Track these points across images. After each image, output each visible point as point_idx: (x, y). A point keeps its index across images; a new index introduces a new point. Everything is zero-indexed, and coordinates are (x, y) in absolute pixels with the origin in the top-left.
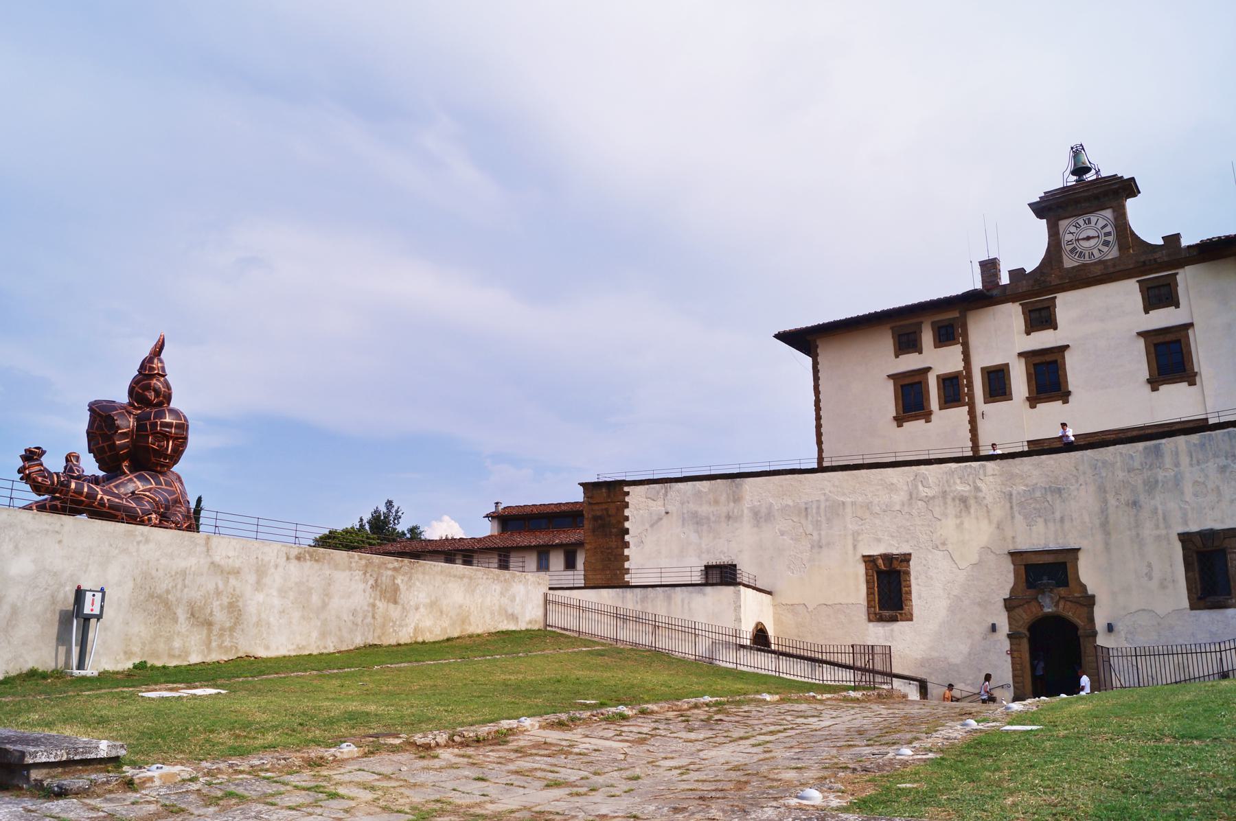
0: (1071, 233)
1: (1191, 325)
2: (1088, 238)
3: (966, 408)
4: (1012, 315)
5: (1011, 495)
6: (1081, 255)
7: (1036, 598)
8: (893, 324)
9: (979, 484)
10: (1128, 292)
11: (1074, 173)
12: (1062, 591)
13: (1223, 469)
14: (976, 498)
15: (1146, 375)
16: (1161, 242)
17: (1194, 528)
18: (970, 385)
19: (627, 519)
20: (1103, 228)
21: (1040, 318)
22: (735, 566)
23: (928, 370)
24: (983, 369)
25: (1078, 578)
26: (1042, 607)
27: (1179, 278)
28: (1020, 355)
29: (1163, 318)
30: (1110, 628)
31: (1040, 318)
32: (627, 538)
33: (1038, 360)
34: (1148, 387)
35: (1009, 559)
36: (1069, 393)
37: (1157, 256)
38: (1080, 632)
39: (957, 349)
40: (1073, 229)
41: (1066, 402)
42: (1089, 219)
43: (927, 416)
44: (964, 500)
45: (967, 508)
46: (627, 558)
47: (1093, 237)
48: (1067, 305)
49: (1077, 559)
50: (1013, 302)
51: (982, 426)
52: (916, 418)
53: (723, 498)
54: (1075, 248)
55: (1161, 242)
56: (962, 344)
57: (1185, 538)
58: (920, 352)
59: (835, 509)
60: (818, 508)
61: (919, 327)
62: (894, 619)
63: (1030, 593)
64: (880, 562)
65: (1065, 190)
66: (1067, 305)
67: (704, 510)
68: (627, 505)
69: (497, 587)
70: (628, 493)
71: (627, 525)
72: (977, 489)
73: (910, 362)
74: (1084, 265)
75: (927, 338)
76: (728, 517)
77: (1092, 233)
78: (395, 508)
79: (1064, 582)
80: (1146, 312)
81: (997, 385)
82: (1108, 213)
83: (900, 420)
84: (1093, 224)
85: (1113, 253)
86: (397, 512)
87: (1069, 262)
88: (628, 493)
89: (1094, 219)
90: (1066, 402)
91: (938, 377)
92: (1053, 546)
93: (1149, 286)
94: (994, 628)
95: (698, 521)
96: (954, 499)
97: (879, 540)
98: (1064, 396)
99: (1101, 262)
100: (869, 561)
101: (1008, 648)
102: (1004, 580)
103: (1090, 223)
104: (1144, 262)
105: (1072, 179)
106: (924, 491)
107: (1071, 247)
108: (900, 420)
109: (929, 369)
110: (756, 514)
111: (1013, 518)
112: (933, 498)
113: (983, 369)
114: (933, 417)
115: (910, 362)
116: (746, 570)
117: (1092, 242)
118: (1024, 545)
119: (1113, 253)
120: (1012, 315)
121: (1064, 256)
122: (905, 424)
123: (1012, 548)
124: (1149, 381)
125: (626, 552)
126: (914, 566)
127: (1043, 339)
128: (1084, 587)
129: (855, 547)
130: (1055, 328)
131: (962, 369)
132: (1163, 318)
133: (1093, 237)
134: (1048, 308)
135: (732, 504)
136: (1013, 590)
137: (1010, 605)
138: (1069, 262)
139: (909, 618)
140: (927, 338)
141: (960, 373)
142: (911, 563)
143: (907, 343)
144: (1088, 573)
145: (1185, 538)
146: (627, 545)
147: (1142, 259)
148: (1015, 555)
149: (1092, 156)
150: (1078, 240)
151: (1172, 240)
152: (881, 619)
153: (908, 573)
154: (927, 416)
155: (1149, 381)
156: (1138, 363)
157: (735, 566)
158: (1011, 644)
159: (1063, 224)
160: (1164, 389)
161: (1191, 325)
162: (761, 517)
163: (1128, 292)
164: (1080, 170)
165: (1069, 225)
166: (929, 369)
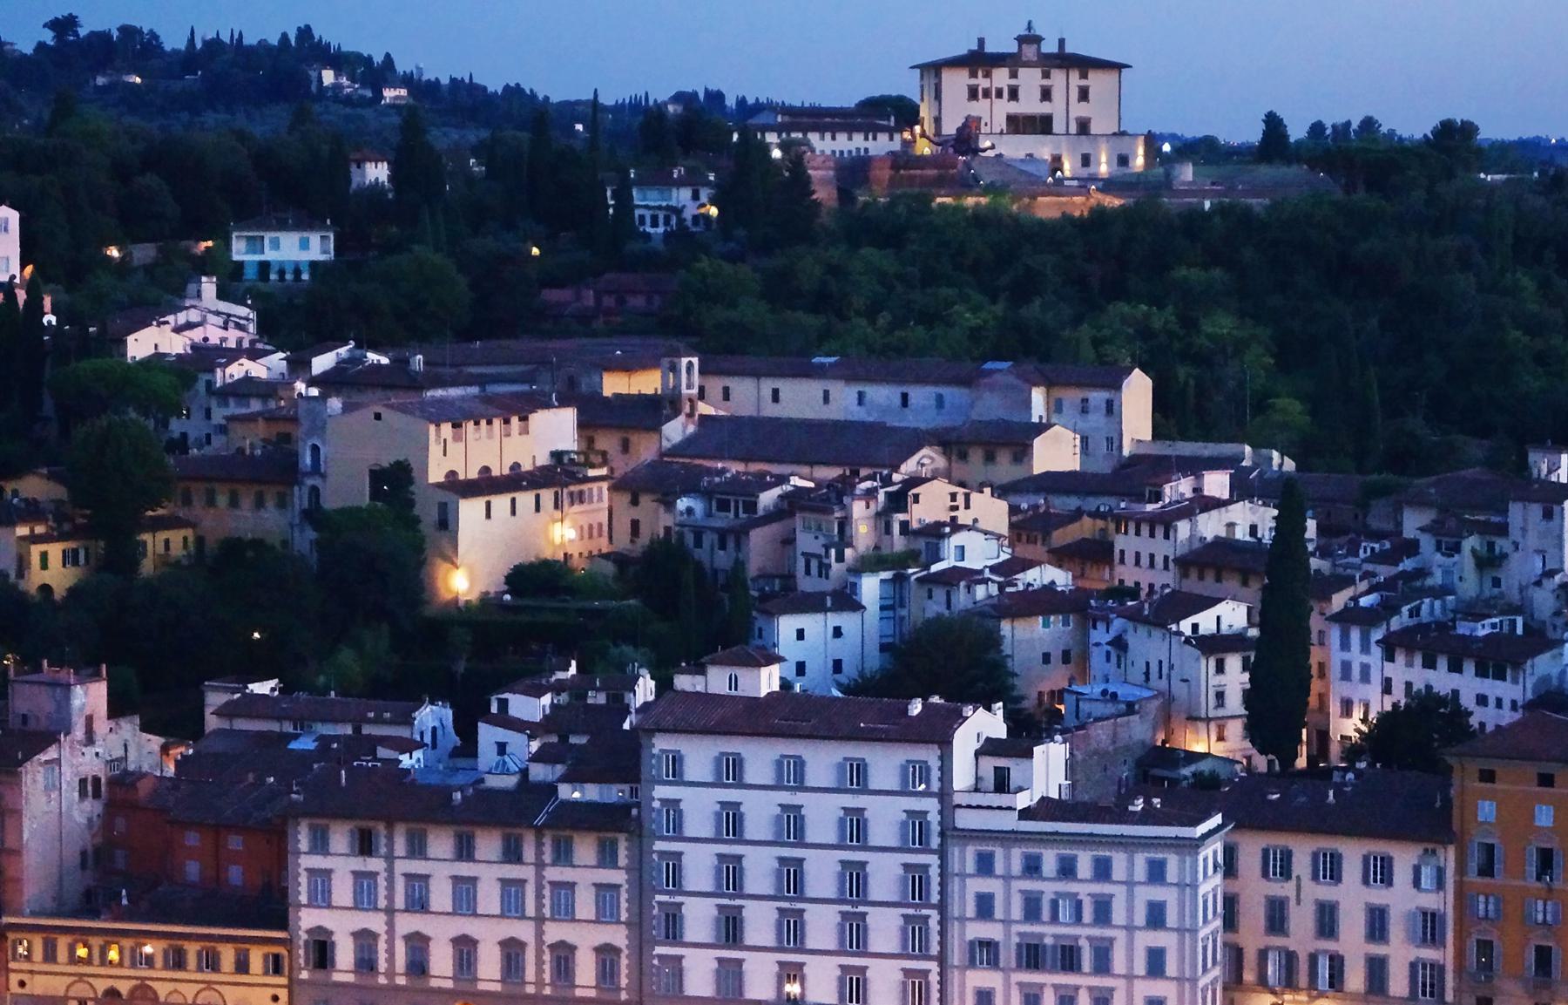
10: (1037, 72)
15: (1039, 97)
21: (1014, 75)
23: (978, 85)
29: (1046, 82)
31: (1014, 75)
48: (1022, 72)
65: (1026, 36)
66: (1022, 72)
73: (973, 81)
81: (999, 94)
82: (1036, 46)
87: (1024, 59)
98: (1017, 100)
105: (1027, 33)
115: (973, 81)
127: (1013, 82)
132: (1046, 82)
138: (1024, 59)
140: (980, 73)
143: (973, 75)
149: (1034, 24)
156: (1038, 95)
163: (1037, 72)
164: (1029, 28)
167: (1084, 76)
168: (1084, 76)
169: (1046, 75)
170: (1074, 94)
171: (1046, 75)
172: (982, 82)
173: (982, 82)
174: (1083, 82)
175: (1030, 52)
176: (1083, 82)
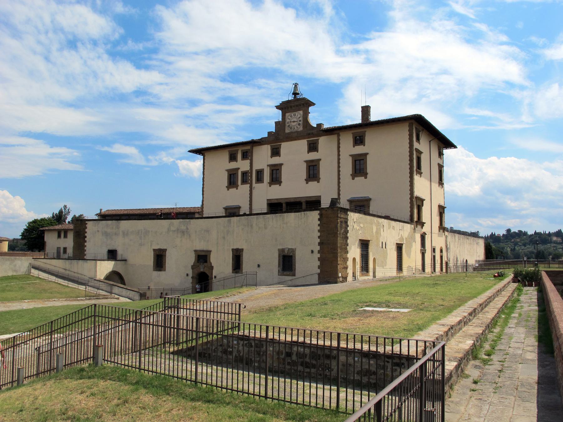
0: (289, 119)
1: (320, 160)
2: (294, 122)
3: (249, 185)
4: (266, 149)
5: (196, 231)
6: (291, 128)
7: (199, 266)
8: (228, 150)
9: (188, 227)
10: (303, 144)
11: (293, 94)
12: (206, 264)
13: (243, 229)
14: (187, 231)
15: (305, 176)
16: (315, 126)
17: (235, 247)
18: (251, 176)
19: (86, 232)
20: (299, 118)
21: (276, 152)
22: (116, 250)
24: (256, 170)
25: (210, 261)
26: (200, 269)
27: (319, 140)
28: (268, 165)
29: (313, 156)
30: (215, 277)
31: (276, 152)
32: (86, 239)
33: (273, 168)
34: (305, 182)
35: (193, 253)
36: (281, 182)
37: (313, 131)
38: (209, 278)
39: (248, 162)
40: (290, 117)
41: (280, 185)
42: (295, 114)
43: (237, 187)
44: (183, 232)
45: (184, 235)
46: (86, 246)
47: (296, 121)
48: (285, 147)
49: (210, 254)
50: (268, 144)
51: (254, 192)
52: (233, 187)
53: (114, 227)
54: (289, 126)
55: (315, 126)
56: (250, 160)
57: (233, 250)
58: (237, 162)
59: (147, 232)
60: (142, 232)
61: (237, 151)
62: (160, 270)
63: (198, 264)
64: (157, 251)
65: (288, 102)
66: (285, 147)
67: (109, 230)
68: (86, 228)
69: (8, 263)
70: (87, 224)
71: (86, 235)
72: (187, 229)
73: (233, 165)
74: (292, 132)
75: (239, 156)
76: (116, 234)
77: (295, 120)
78: (68, 208)
79: (206, 262)
80: (308, 153)
82: (301, 112)
83: (228, 188)
84: (296, 116)
85: (301, 128)
86: (68, 210)
87: (287, 131)
88: (87, 224)
89: (297, 114)
90: (280, 185)
91: (241, 172)
92: (205, 249)
93: (310, 143)
94: (187, 275)
95: (106, 234)
96: (180, 232)
97: (158, 244)
99: (297, 132)
100: (154, 250)
101: (191, 281)
102: (191, 259)
103: (295, 115)
104: (309, 133)
105: (291, 98)
106: (172, 228)
107: (288, 124)
108: (228, 188)
109: (239, 169)
110: (123, 233)
111: (196, 239)
112: (175, 231)
113: (256, 170)
114: (239, 188)
115: (233, 165)
116: (120, 252)
117: (295, 123)
118: (198, 248)
119: (301, 128)
120: (266, 149)
121: (286, 128)
122: (230, 189)
123: (195, 249)
124: (306, 180)
125: (86, 244)
126: (168, 254)
127: (276, 160)
128: (211, 263)
129: (151, 246)
130: (280, 156)
131: (249, 169)
132: (313, 156)
133: (296, 121)
134: (279, 148)
135: (117, 229)
136: (194, 263)
137: (193, 267)
138: (287, 131)
139: (165, 270)
140: (239, 156)
141: (249, 171)
142: (167, 252)
143: (233, 158)
144: (213, 259)
145: (233, 250)
146: (86, 242)
147: (309, 132)
148: (195, 251)
150: (291, 122)
151: (319, 125)
152: (156, 270)
153: (165, 256)
154: (237, 187)
155: (306, 180)
157: (116, 250)
158: (192, 280)
159: (287, 114)
160: (310, 183)
161: (320, 160)
162: (125, 234)
163: (303, 144)
164: (295, 94)
165: (288, 116)
166: (239, 169)
167: (359, 141)
168: (359, 141)
169: (313, 147)
170: (347, 167)
171: (313, 147)
172: (243, 165)
173: (243, 165)
174: (359, 150)
175: (294, 119)
176: (359, 150)
